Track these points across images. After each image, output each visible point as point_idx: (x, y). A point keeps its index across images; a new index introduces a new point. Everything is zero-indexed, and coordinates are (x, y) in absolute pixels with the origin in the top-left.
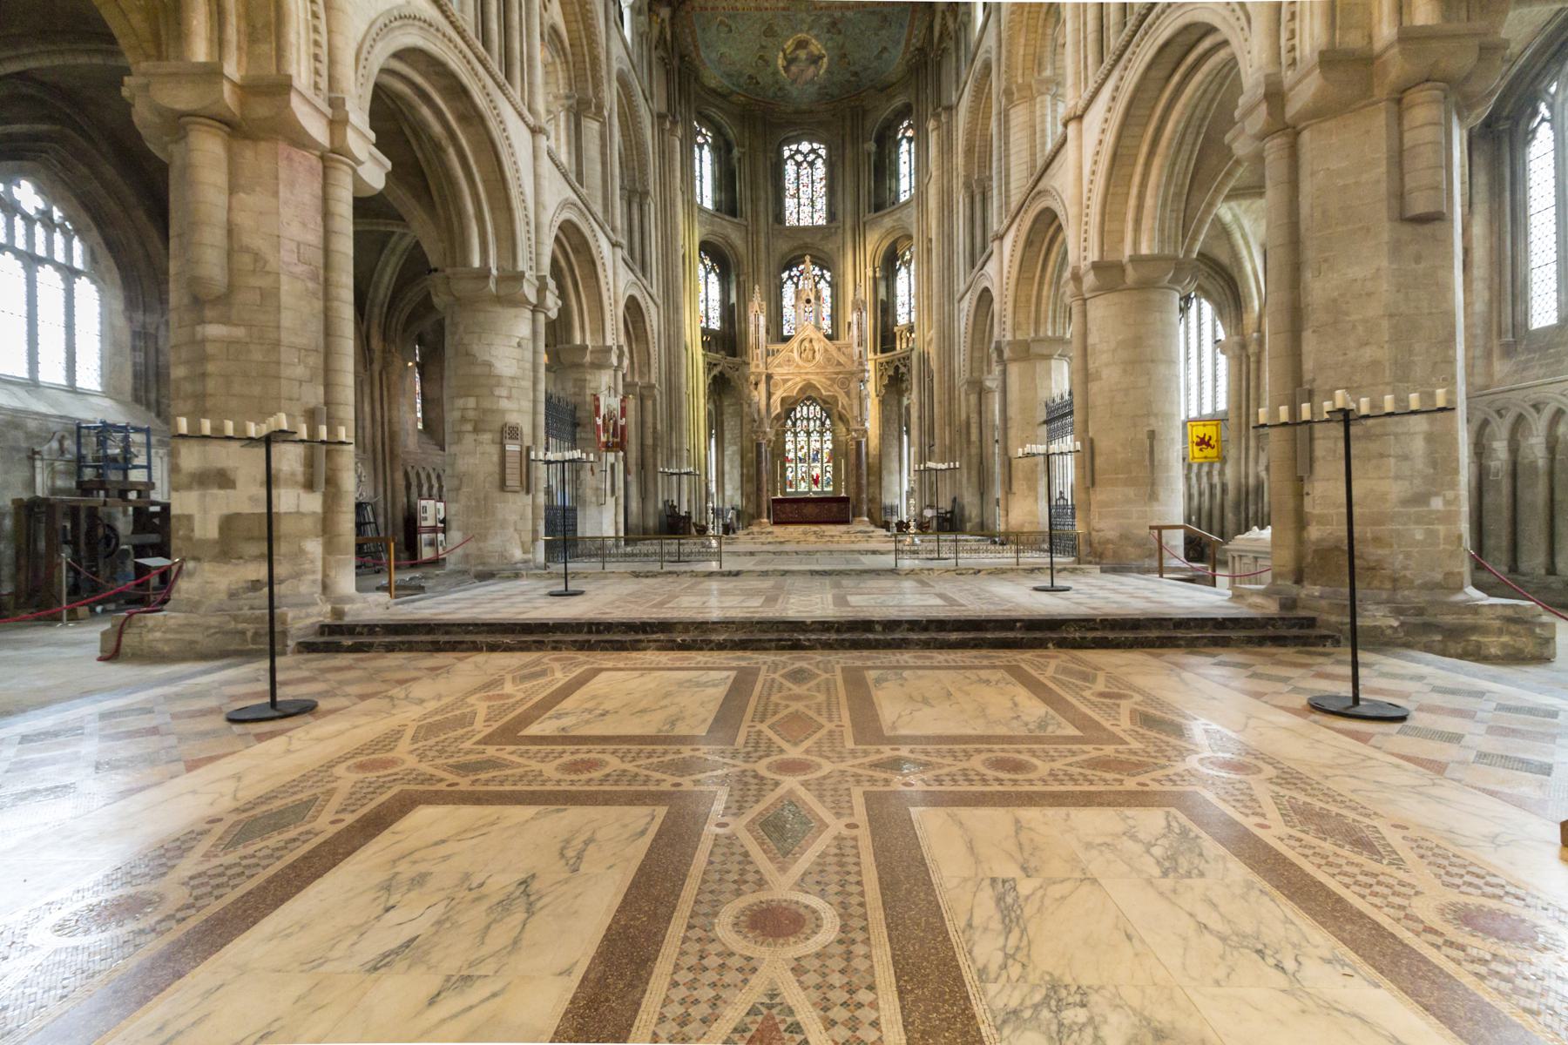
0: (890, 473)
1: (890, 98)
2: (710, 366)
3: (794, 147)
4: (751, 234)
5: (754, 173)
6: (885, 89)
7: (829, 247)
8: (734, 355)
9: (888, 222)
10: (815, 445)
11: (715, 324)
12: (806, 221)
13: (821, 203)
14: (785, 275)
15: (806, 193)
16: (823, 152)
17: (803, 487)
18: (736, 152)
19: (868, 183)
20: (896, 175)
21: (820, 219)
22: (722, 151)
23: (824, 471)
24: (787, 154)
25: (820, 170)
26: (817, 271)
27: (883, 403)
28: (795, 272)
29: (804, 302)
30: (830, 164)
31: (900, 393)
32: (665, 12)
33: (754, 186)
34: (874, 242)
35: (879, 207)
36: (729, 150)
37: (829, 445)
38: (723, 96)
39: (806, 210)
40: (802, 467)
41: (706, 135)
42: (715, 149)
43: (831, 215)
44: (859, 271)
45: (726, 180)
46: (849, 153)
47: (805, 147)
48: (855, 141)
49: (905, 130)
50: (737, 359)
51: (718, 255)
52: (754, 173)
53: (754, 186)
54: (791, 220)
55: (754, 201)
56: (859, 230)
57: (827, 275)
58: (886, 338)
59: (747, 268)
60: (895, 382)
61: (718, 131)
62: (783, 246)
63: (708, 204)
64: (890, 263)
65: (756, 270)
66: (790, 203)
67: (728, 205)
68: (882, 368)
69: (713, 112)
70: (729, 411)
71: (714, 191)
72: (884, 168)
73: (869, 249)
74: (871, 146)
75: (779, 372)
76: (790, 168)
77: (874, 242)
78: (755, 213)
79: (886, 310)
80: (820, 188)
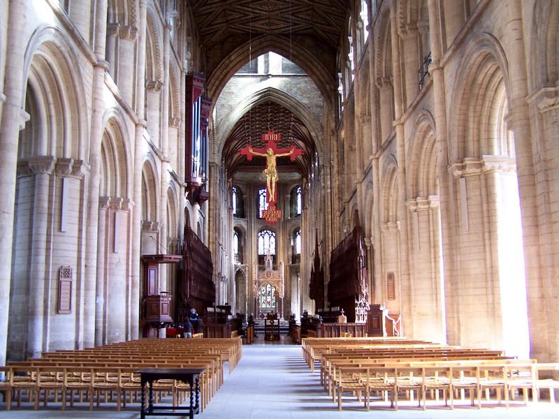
0: (294, 304)
1: (295, 183)
3: (263, 191)
6: (294, 181)
7: (274, 227)
10: (269, 289)
14: (260, 234)
17: (264, 306)
18: (245, 196)
20: (296, 204)
23: (272, 300)
26: (270, 233)
28: (263, 233)
32: (230, 180)
36: (242, 194)
37: (274, 289)
38: (242, 181)
40: (264, 298)
42: (236, 194)
45: (241, 204)
46: (282, 199)
48: (284, 195)
50: (244, 265)
51: (239, 232)
55: (251, 213)
57: (274, 234)
61: (238, 188)
69: (238, 185)
71: (237, 207)
72: (293, 202)
73: (288, 229)
74: (289, 196)
78: (251, 216)
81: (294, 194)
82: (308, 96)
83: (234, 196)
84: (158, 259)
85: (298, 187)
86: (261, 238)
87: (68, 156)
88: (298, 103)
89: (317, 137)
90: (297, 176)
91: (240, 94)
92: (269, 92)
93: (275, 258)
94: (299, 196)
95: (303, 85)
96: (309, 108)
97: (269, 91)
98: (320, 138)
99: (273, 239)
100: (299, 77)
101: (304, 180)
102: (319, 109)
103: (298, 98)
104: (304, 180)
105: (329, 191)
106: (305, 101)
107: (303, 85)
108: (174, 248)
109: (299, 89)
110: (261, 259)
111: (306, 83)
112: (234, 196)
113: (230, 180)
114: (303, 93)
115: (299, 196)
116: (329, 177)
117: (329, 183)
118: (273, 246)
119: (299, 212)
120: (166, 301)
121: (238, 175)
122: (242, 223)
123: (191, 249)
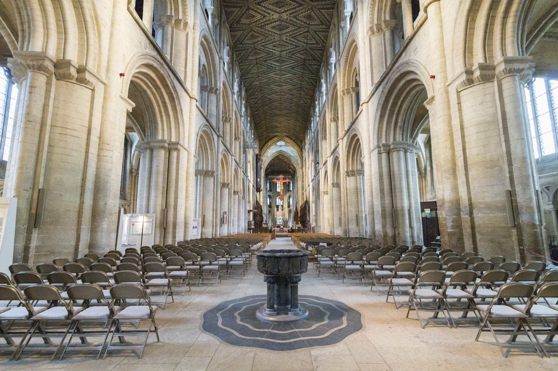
4: (273, 193)
44: (286, 198)
45: (270, 187)
51: (270, 196)
64: (289, 197)
67: (270, 190)
77: (288, 195)
79: (289, 203)
84: (251, 211)
87: (209, 169)
88: (290, 155)
90: (290, 177)
91: (271, 152)
93: (282, 206)
106: (292, 155)
108: (254, 208)
110: (278, 207)
120: (253, 222)
121: (269, 177)
122: (271, 194)
123: (258, 207)
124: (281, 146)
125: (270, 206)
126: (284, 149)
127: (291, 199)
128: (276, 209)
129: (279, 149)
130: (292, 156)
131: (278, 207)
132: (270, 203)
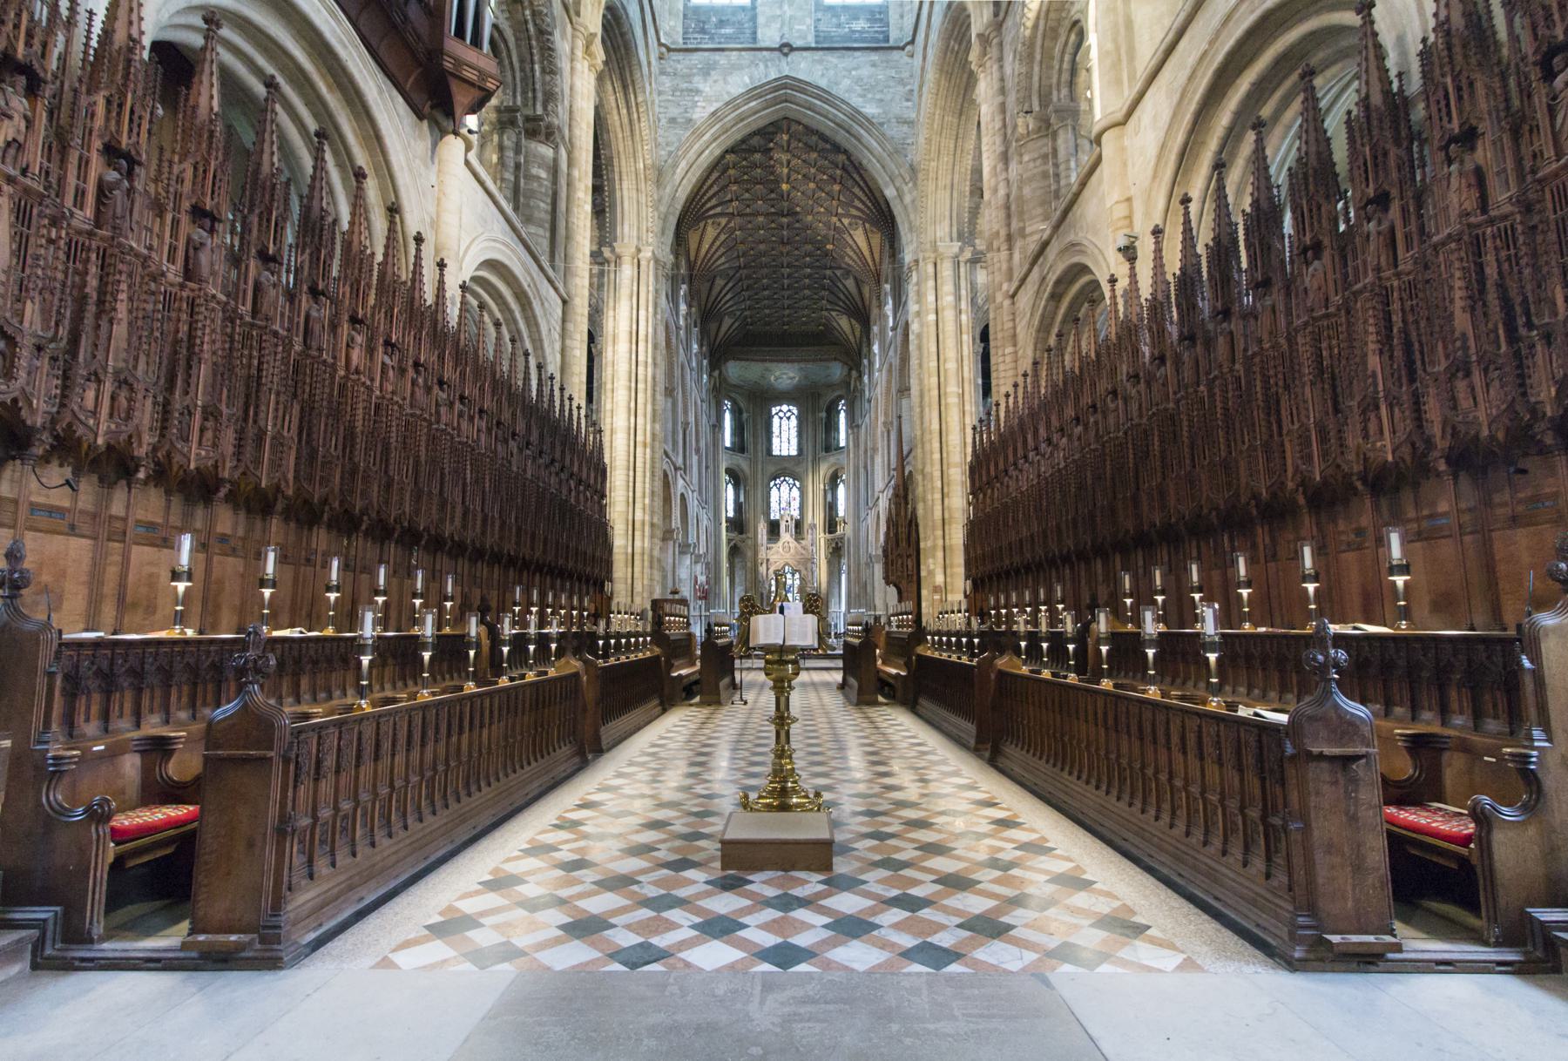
2: (729, 541)
4: (753, 462)
5: (755, 426)
6: (830, 386)
8: (741, 533)
9: (832, 460)
11: (731, 514)
12: (785, 453)
13: (794, 441)
15: (785, 434)
16: (795, 411)
18: (745, 415)
19: (821, 436)
20: (837, 430)
21: (794, 452)
22: (737, 413)
24: (774, 410)
25: (794, 421)
27: (829, 563)
29: (783, 498)
30: (798, 418)
31: (840, 557)
32: (716, 373)
33: (755, 436)
34: (824, 470)
35: (828, 449)
37: (797, 582)
39: (785, 445)
41: (728, 404)
42: (733, 412)
43: (800, 449)
44: (816, 484)
45: (738, 430)
47: (785, 408)
48: (814, 413)
49: (842, 405)
51: (736, 477)
52: (755, 426)
53: (755, 436)
54: (776, 452)
55: (755, 444)
56: (816, 461)
58: (831, 525)
59: (750, 482)
60: (836, 551)
61: (734, 402)
62: (771, 469)
63: (728, 444)
65: (755, 484)
66: (775, 441)
67: (739, 447)
68: (829, 542)
70: (738, 566)
72: (831, 426)
74: (824, 415)
75: (773, 558)
76: (776, 420)
77: (824, 470)
79: (831, 507)
80: (794, 433)
81: (832, 411)
82: (878, 96)
83: (727, 416)
85: (840, 398)
86: (774, 492)
88: (856, 115)
89: (900, 196)
90: (837, 371)
92: (786, 88)
93: (799, 525)
94: (842, 415)
95: (865, 72)
96: (882, 124)
97: (785, 86)
98: (908, 199)
99: (796, 493)
100: (858, 54)
101: (854, 373)
102: (905, 128)
103: (856, 101)
104: (854, 373)
105: (932, 317)
106: (870, 110)
107: (865, 72)
109: (858, 80)
111: (874, 65)
112: (727, 416)
113: (716, 373)
114: (868, 89)
115: (842, 415)
116: (931, 283)
117: (931, 298)
118: (796, 504)
119: (842, 443)
124: (786, 49)
125: (738, 525)
126: (804, 68)
127: (841, 490)
128: (762, 530)
129: (770, 70)
130: (867, 123)
131: (774, 528)
132: (738, 507)
